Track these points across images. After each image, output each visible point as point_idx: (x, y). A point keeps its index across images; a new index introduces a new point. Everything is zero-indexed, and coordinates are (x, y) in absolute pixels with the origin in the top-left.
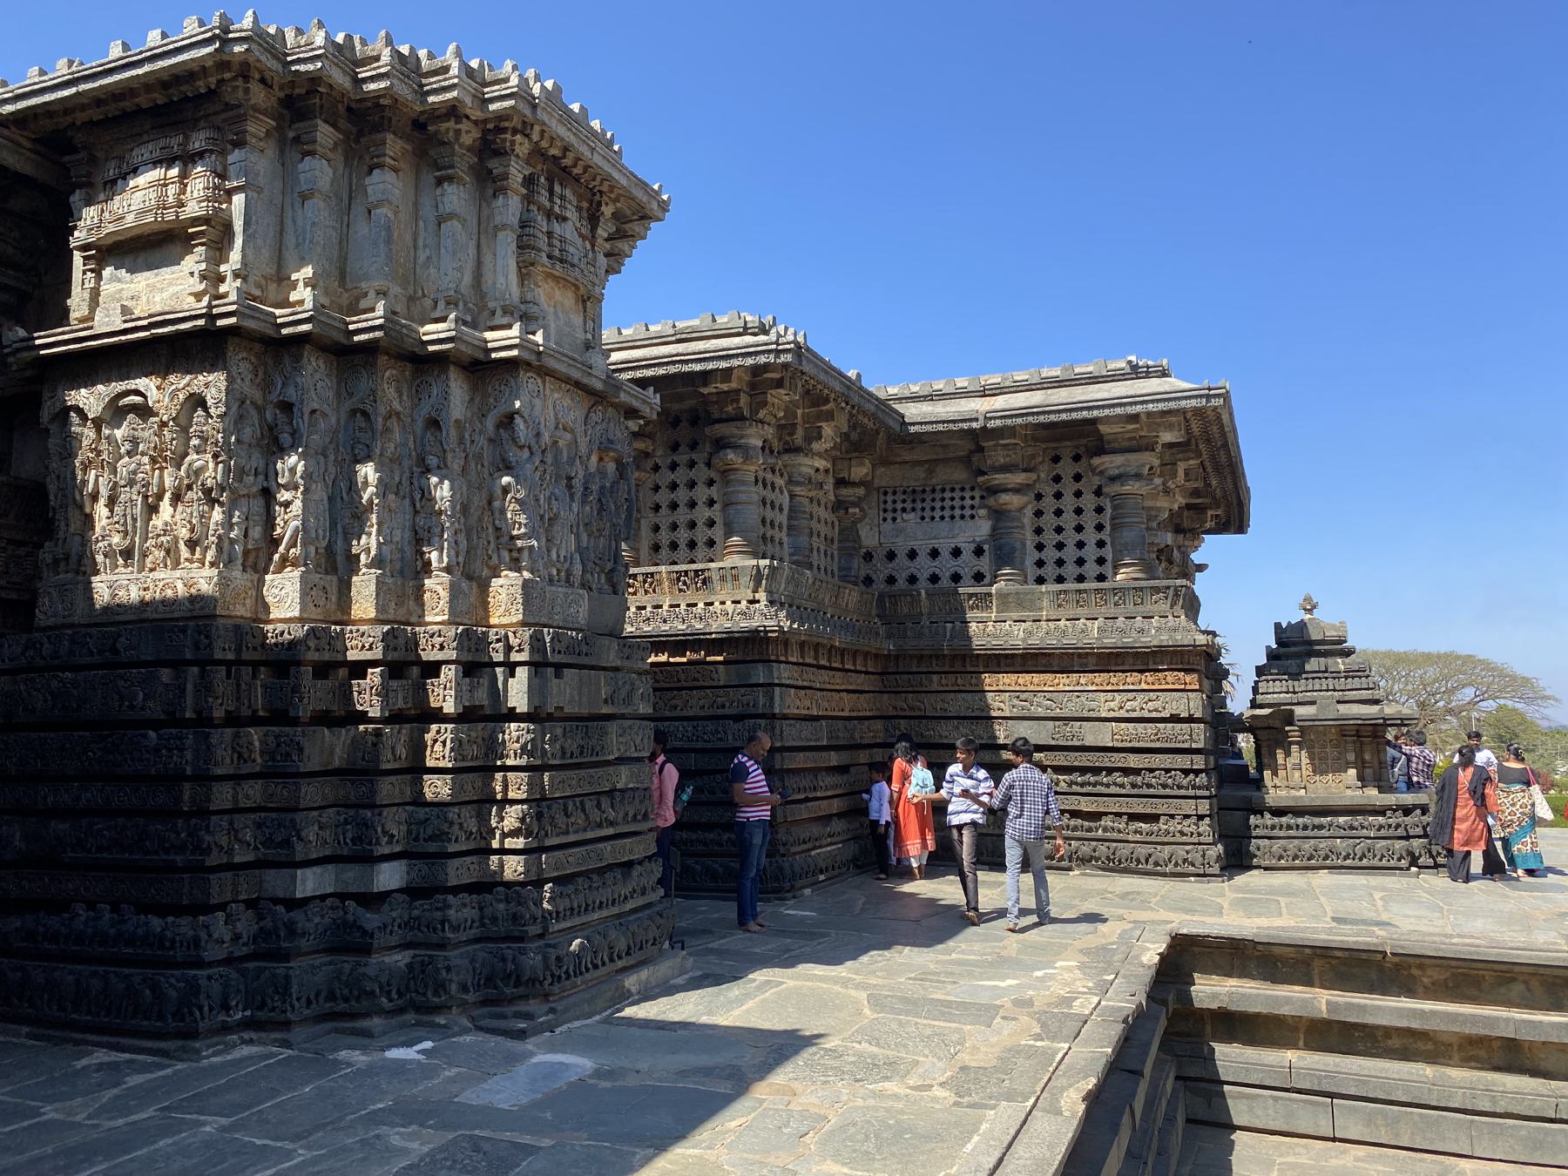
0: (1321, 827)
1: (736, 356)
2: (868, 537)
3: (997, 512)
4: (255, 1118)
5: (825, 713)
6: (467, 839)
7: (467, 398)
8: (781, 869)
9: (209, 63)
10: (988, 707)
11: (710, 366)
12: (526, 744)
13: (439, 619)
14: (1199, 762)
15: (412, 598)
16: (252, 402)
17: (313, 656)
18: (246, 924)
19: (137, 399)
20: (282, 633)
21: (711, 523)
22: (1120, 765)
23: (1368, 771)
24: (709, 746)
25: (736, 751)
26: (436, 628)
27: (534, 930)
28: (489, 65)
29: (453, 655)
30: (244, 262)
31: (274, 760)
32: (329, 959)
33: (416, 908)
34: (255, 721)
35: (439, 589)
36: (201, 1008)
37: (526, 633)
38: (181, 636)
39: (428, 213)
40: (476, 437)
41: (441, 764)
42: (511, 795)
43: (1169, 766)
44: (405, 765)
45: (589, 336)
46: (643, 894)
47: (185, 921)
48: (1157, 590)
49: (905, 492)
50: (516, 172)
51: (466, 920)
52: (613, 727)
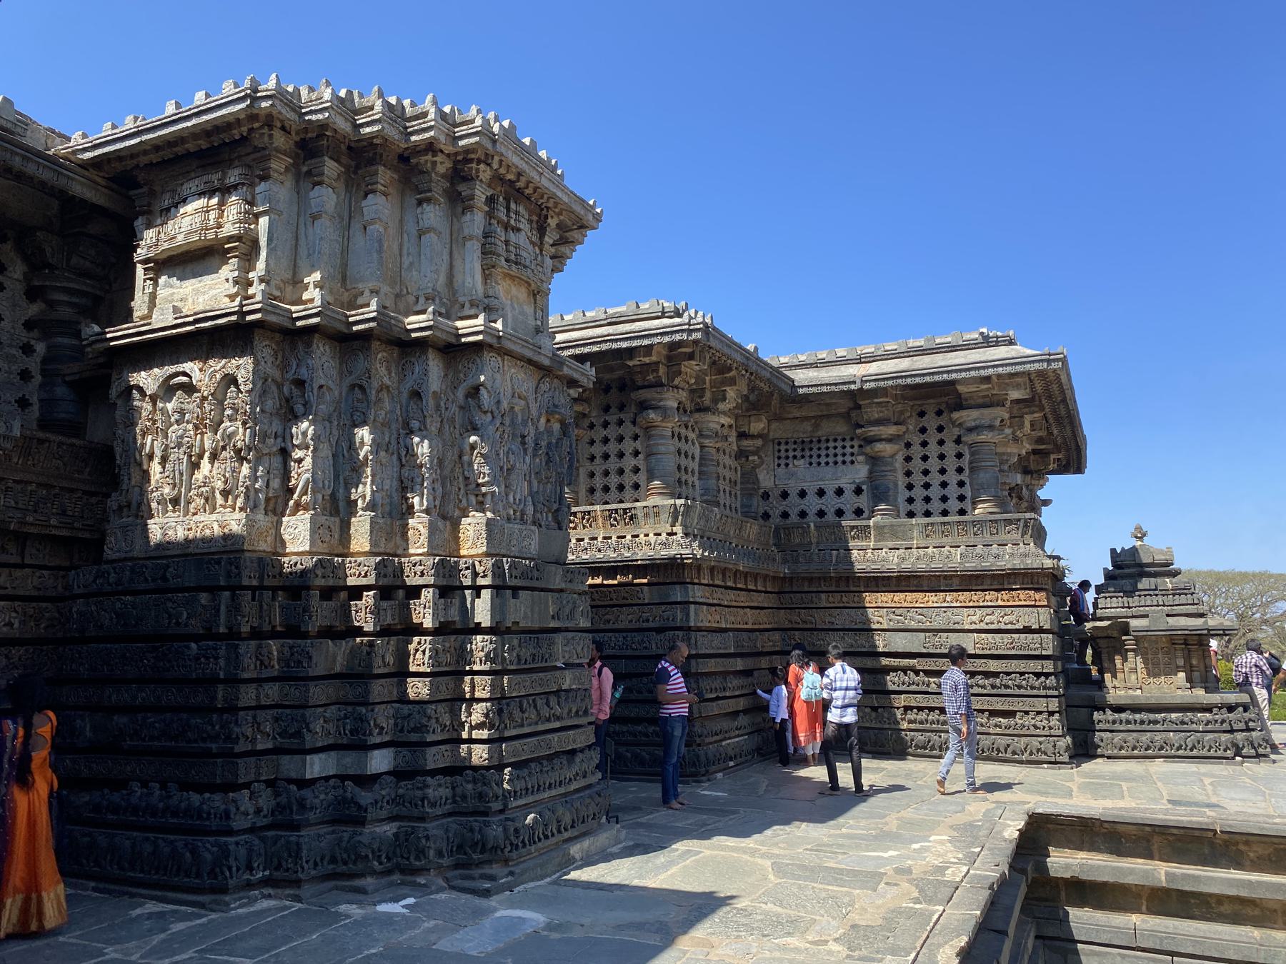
0: (1156, 722)
1: (657, 335)
2: (766, 480)
3: (872, 458)
4: (273, 960)
5: (732, 626)
6: (442, 730)
7: (442, 374)
8: (698, 756)
9: (242, 116)
10: (869, 621)
11: (635, 343)
12: (489, 653)
13: (420, 551)
14: (1049, 666)
17: (320, 582)
18: (266, 800)
19: (184, 379)
20: (296, 564)
21: (636, 470)
22: (981, 669)
23: (1196, 675)
24: (637, 653)
25: (660, 657)
26: (418, 558)
27: (496, 806)
28: (459, 110)
29: (431, 580)
30: (268, 270)
31: (289, 666)
32: (331, 829)
33: (401, 787)
34: (274, 635)
35: (420, 527)
36: (230, 869)
37: (489, 562)
39: (411, 228)
40: (450, 405)
41: (421, 669)
42: (478, 695)
43: (1023, 670)
45: (539, 323)
46: (584, 777)
47: (217, 797)
48: (1010, 522)
49: (795, 443)
50: (481, 194)
51: (441, 798)
52: (559, 638)
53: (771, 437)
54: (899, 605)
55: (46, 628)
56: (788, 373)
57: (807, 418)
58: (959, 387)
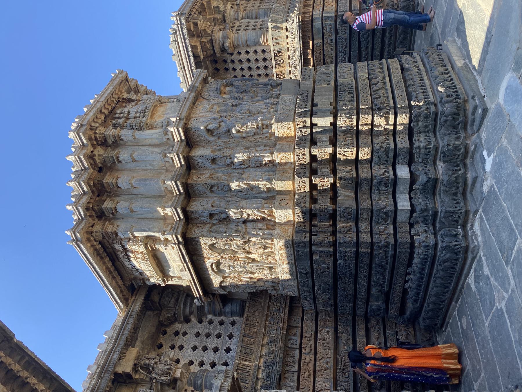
1: (185, 42)
4: (520, 228)
6: (388, 140)
7: (202, 148)
8: (404, 6)
11: (191, 54)
12: (347, 117)
13: (292, 156)
15: (284, 167)
16: (211, 228)
17: (308, 205)
18: (420, 228)
20: (299, 216)
21: (256, 52)
24: (348, 45)
25: (351, 28)
26: (296, 157)
30: (159, 232)
31: (350, 218)
32: (438, 196)
33: (418, 161)
34: (334, 225)
35: (280, 157)
36: (456, 245)
37: (298, 119)
38: (300, 252)
39: (133, 165)
40: (218, 144)
42: (370, 122)
45: (175, 100)
46: (416, 62)
47: (416, 251)
50: (111, 132)
51: (426, 139)
52: (340, 80)
55: (330, 317)
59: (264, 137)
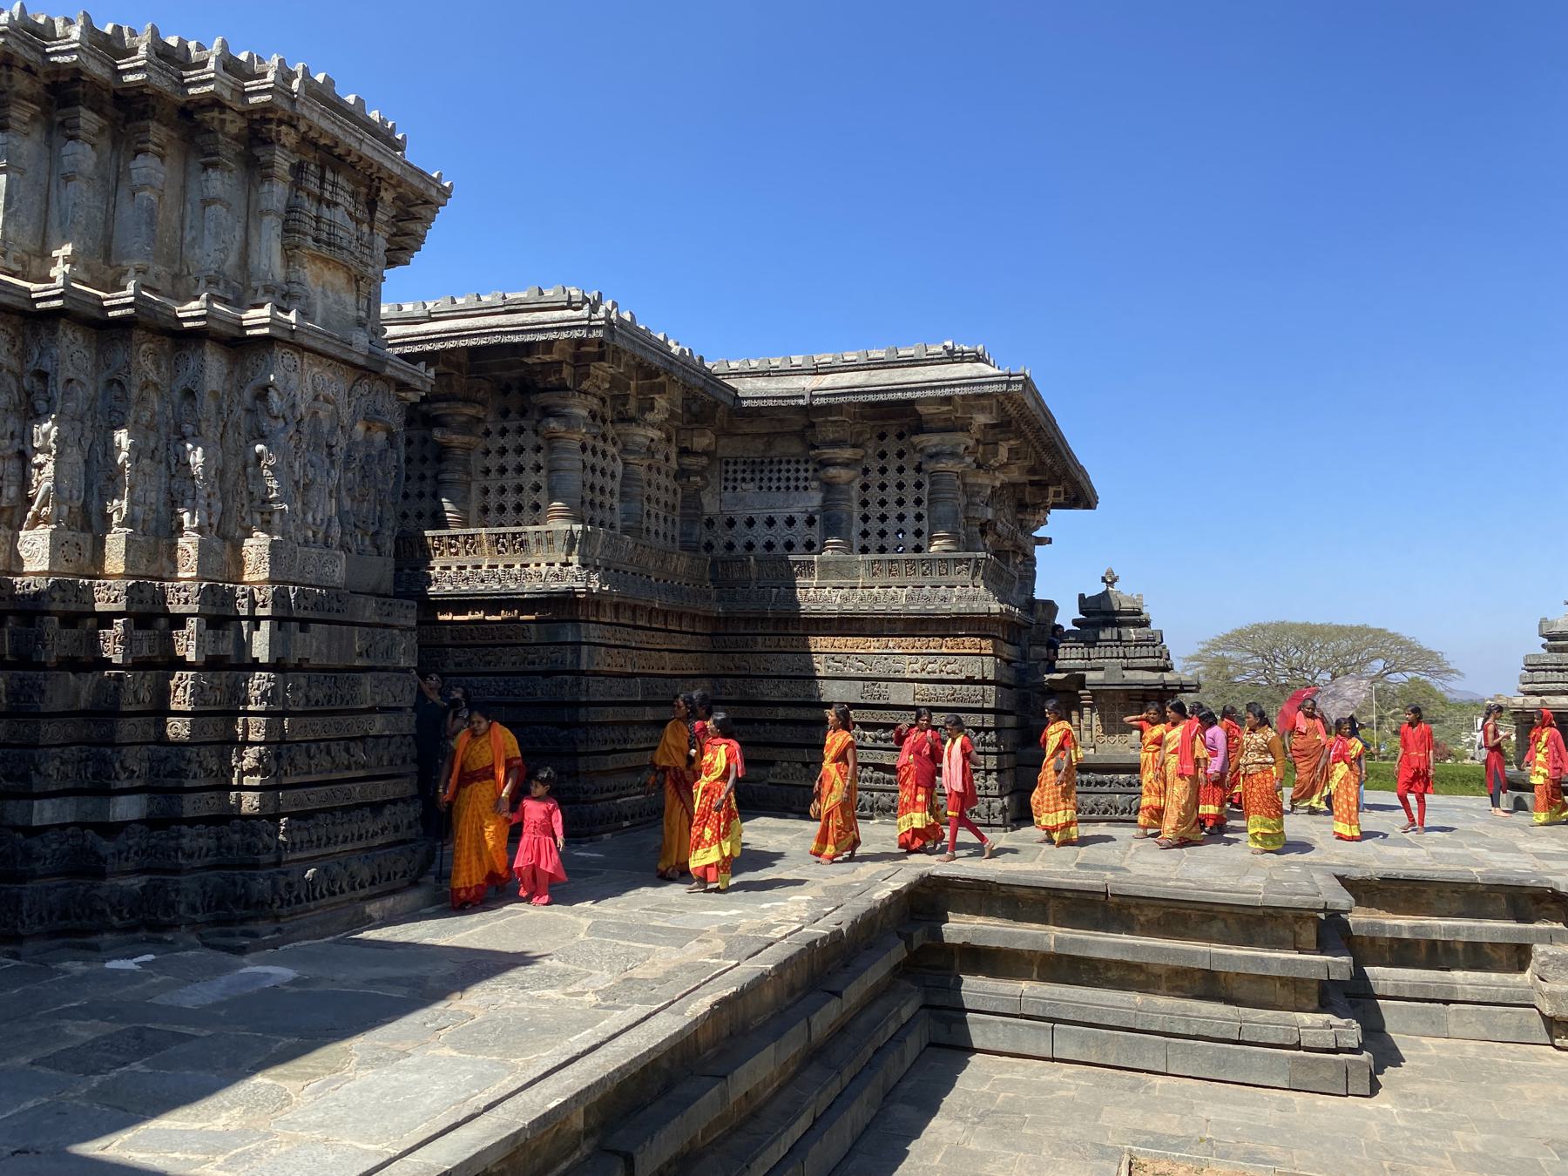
0: (1102, 783)
1: (552, 329)
2: (710, 505)
3: (827, 484)
5: (641, 671)
11: (529, 338)
13: (188, 575)
14: (990, 721)
16: (9, 371)
21: (537, 488)
26: (182, 583)
27: (266, 858)
28: (258, 57)
29: (196, 609)
32: (66, 882)
35: (190, 547)
37: (269, 590)
40: (234, 407)
41: (182, 707)
42: (251, 737)
44: (149, 708)
45: (363, 314)
48: (959, 561)
49: (745, 463)
50: (282, 162)
51: (201, 848)
53: (718, 456)
54: (839, 651)
56: (732, 383)
57: (759, 435)
58: (918, 408)
59: (243, 514)
